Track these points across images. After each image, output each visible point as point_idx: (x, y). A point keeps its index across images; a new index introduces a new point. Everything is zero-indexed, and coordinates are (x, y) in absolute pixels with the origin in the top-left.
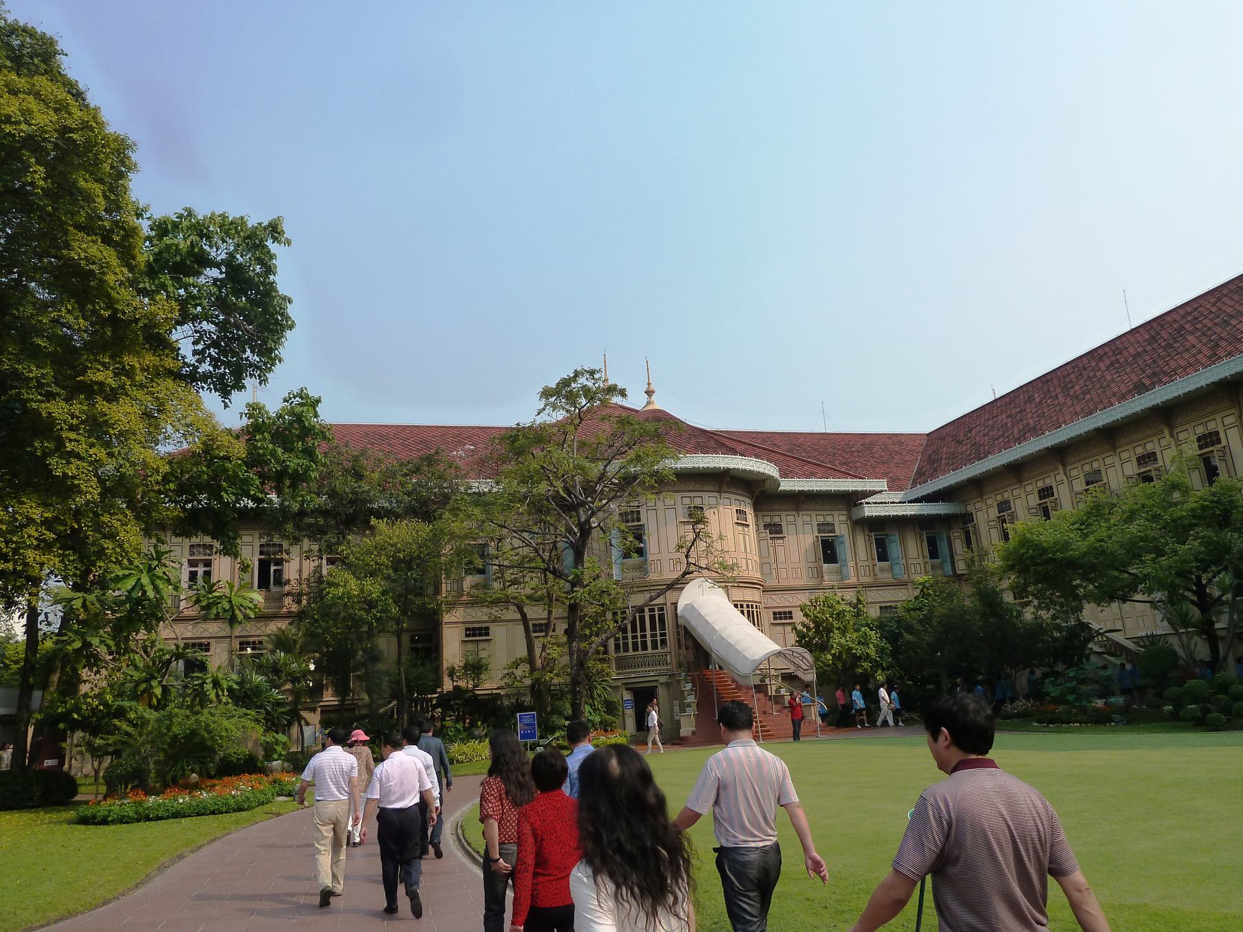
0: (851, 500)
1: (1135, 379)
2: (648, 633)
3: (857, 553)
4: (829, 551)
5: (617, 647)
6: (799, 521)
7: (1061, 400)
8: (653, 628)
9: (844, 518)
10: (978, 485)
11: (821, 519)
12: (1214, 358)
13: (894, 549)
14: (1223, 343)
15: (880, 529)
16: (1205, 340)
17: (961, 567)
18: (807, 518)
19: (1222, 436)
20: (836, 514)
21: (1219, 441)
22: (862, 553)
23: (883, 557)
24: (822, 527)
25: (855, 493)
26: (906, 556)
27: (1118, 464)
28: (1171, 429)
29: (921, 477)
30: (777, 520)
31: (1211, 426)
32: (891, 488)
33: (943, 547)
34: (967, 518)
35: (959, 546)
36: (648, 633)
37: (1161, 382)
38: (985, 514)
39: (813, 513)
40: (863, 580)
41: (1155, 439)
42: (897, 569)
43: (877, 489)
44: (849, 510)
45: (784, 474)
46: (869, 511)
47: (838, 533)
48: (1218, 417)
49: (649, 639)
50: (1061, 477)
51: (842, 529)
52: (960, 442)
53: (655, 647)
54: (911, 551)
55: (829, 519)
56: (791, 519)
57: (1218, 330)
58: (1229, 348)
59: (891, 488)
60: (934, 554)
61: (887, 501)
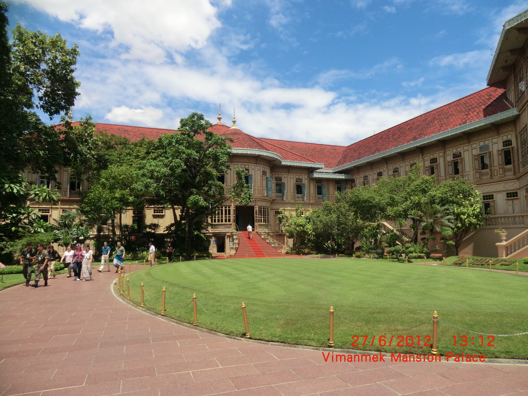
0: (311, 170)
1: (415, 135)
2: (224, 216)
3: (310, 190)
4: (299, 189)
5: (219, 220)
6: (289, 176)
7: (391, 139)
8: (226, 214)
9: (306, 177)
11: (297, 177)
13: (324, 191)
14: (444, 125)
16: (440, 123)
18: (292, 176)
19: (438, 160)
20: (303, 175)
21: (437, 161)
22: (312, 191)
23: (320, 192)
24: (297, 180)
25: (311, 168)
26: (329, 194)
27: (404, 166)
28: (423, 155)
29: (340, 163)
30: (280, 176)
31: (435, 156)
36: (224, 216)
37: (421, 137)
39: (295, 174)
40: (311, 202)
41: (417, 158)
43: (320, 167)
44: (309, 174)
45: (285, 158)
46: (316, 175)
47: (303, 183)
48: (438, 153)
49: (224, 218)
50: (385, 169)
51: (305, 181)
52: (355, 151)
53: (226, 221)
55: (301, 177)
56: (286, 176)
57: (445, 120)
58: (445, 128)
59: (326, 167)
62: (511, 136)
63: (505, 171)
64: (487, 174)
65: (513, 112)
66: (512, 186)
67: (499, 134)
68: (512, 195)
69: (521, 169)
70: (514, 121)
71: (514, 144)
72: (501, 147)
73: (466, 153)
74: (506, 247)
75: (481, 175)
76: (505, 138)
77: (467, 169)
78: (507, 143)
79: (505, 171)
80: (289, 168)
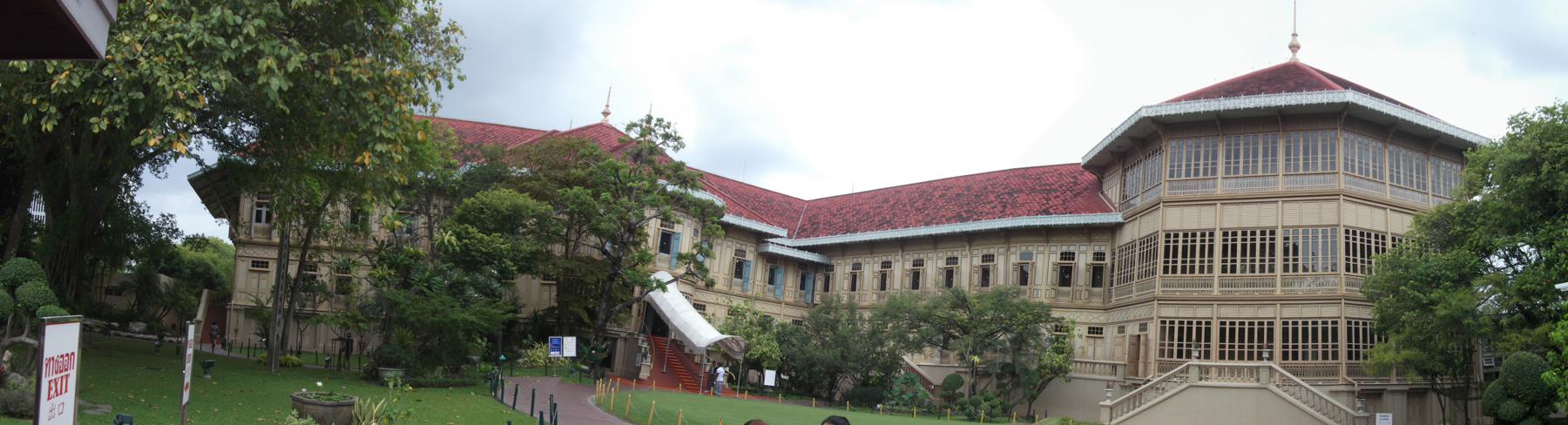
3: (757, 273)
4: (739, 269)
10: (844, 249)
12: (1003, 214)
13: (779, 277)
15: (775, 263)
17: (817, 299)
23: (771, 281)
32: (790, 236)
33: (809, 283)
34: (828, 268)
35: (819, 285)
38: (842, 270)
42: (778, 292)
46: (772, 249)
54: (789, 282)
60: (802, 287)
61: (784, 244)
62: (1105, 248)
63: (1091, 295)
64: (1067, 294)
65: (1116, 218)
66: (1096, 318)
67: (1090, 241)
68: (1095, 331)
69: (1113, 299)
70: (1113, 229)
71: (1108, 260)
72: (1090, 260)
73: (1040, 257)
74: (1111, 408)
75: (1058, 293)
76: (1097, 249)
77: (1038, 281)
78: (1099, 256)
79: (1091, 295)
80: (730, 229)
